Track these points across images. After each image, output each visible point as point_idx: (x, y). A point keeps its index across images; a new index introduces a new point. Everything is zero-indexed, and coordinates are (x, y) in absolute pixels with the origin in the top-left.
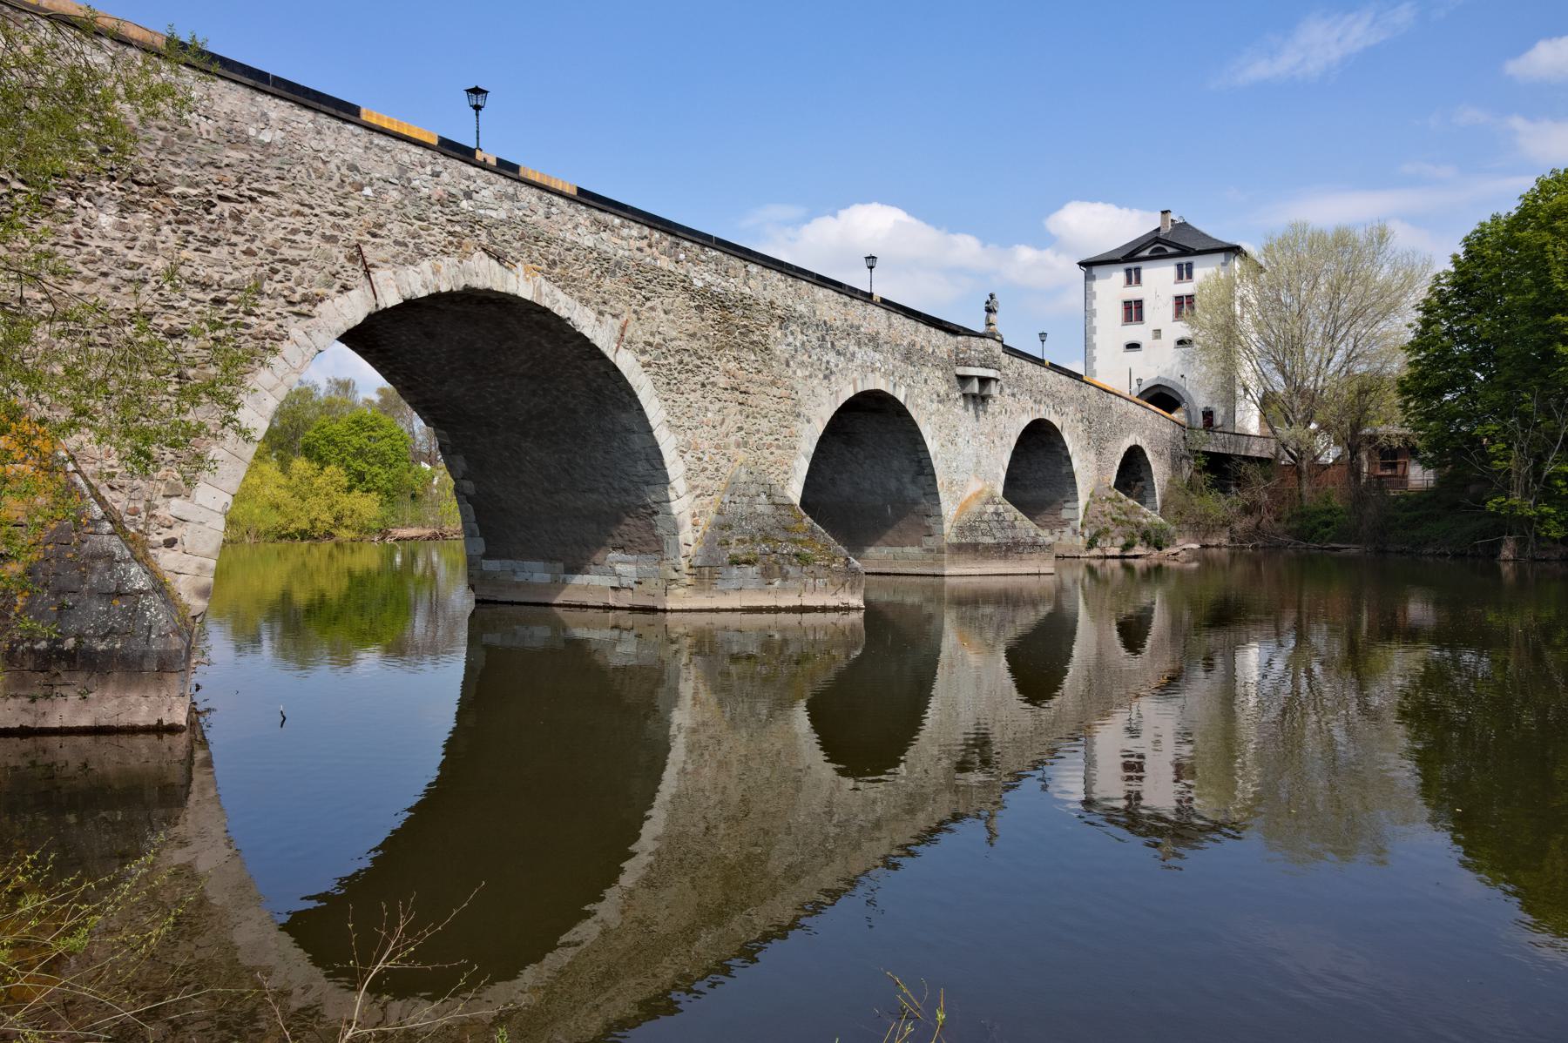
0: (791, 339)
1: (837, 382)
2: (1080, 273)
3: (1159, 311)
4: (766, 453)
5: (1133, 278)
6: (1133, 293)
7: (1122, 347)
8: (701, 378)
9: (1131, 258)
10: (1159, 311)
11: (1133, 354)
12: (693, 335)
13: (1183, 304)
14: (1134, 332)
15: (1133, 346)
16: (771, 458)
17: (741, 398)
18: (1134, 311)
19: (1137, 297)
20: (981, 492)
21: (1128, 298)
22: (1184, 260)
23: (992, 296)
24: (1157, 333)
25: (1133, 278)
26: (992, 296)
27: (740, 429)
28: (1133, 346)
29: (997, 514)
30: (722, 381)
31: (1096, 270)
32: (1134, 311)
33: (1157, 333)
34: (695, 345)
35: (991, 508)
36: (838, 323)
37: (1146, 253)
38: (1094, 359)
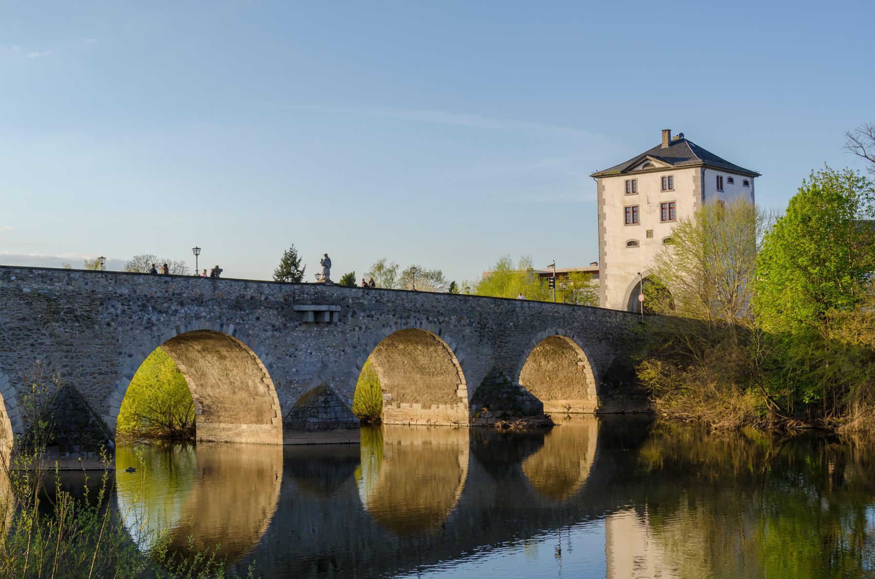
0: (112, 310)
1: (159, 330)
2: (593, 183)
3: (649, 217)
4: (89, 378)
5: (631, 189)
6: (631, 200)
7: (625, 245)
8: (32, 341)
9: (629, 169)
10: (649, 217)
11: (631, 250)
12: (24, 319)
13: (667, 211)
14: (635, 232)
15: (631, 244)
16: (95, 380)
17: (65, 348)
18: (631, 215)
19: (635, 204)
20: (319, 387)
21: (628, 205)
22: (666, 174)
23: (326, 255)
24: (649, 234)
25: (631, 189)
26: (326, 255)
27: (66, 366)
28: (631, 244)
29: (326, 402)
30: (48, 341)
31: (606, 181)
32: (631, 215)
33: (649, 234)
34: (26, 324)
35: (322, 399)
36: (159, 294)
37: (640, 168)
38: (605, 254)
